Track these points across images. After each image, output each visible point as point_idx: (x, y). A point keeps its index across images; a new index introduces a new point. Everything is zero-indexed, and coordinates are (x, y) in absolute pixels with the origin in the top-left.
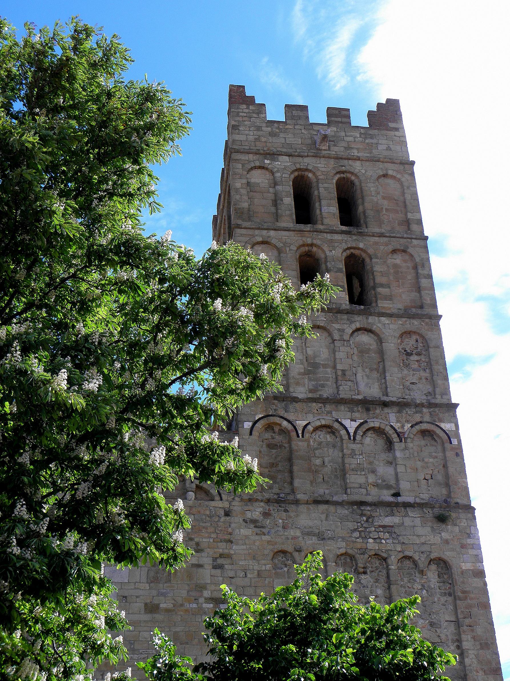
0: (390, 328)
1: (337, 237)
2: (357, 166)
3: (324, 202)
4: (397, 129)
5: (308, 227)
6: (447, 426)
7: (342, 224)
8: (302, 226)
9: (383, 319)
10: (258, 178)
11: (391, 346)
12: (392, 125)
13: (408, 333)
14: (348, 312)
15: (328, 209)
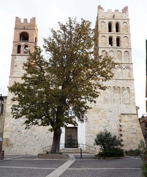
0: (123, 51)
1: (115, 34)
2: (119, 21)
3: (113, 28)
4: (126, 13)
5: (111, 33)
6: (131, 67)
7: (116, 32)
8: (110, 33)
9: (122, 49)
10: (103, 24)
11: (123, 53)
12: (126, 12)
13: (126, 51)
14: (116, 48)
15: (114, 29)
